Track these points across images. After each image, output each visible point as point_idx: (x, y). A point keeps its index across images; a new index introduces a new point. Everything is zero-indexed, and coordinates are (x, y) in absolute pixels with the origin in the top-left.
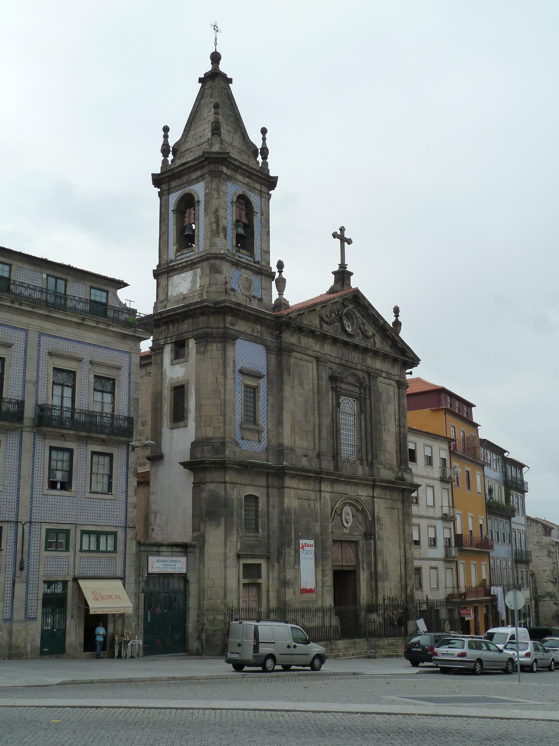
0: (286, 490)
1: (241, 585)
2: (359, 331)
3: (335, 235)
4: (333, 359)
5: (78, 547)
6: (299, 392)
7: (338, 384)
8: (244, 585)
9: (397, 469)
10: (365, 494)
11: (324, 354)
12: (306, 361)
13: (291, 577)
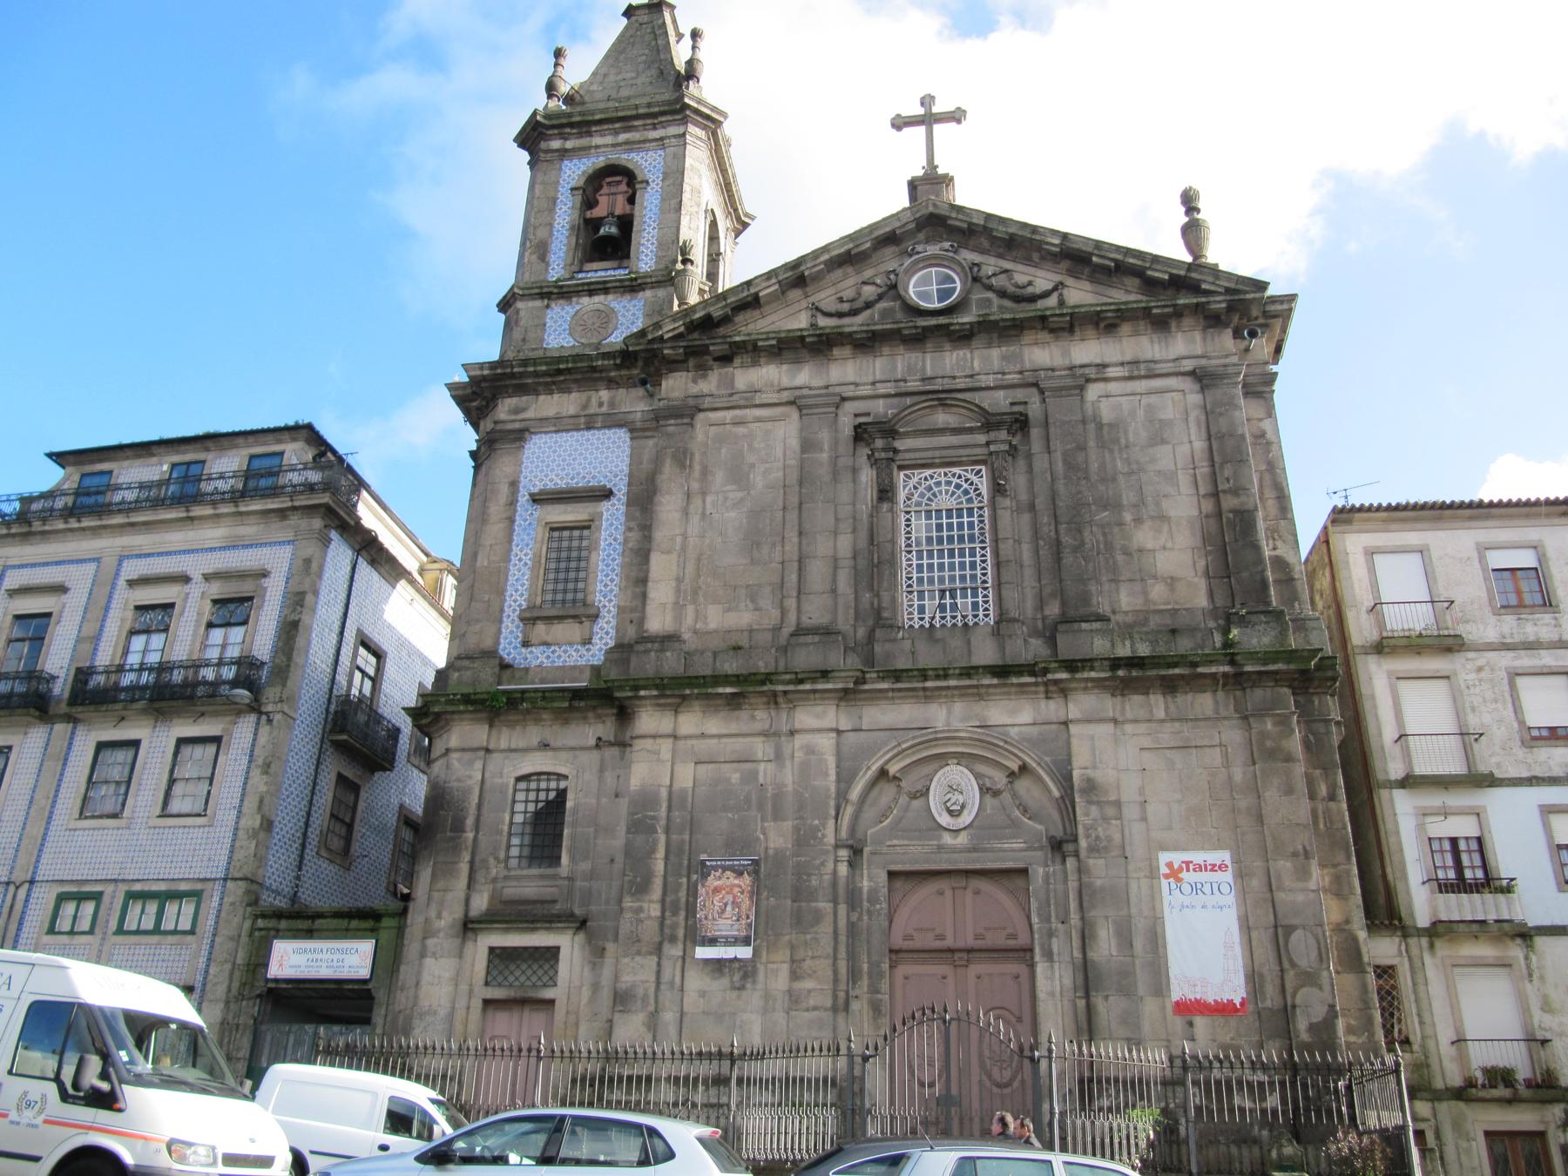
0: (639, 744)
1: (477, 1004)
2: (990, 295)
3: (900, 123)
4: (866, 391)
5: (113, 925)
6: (726, 499)
7: (879, 443)
8: (487, 1003)
9: (1212, 624)
10: (1026, 716)
11: (827, 387)
12: (759, 420)
13: (643, 978)
